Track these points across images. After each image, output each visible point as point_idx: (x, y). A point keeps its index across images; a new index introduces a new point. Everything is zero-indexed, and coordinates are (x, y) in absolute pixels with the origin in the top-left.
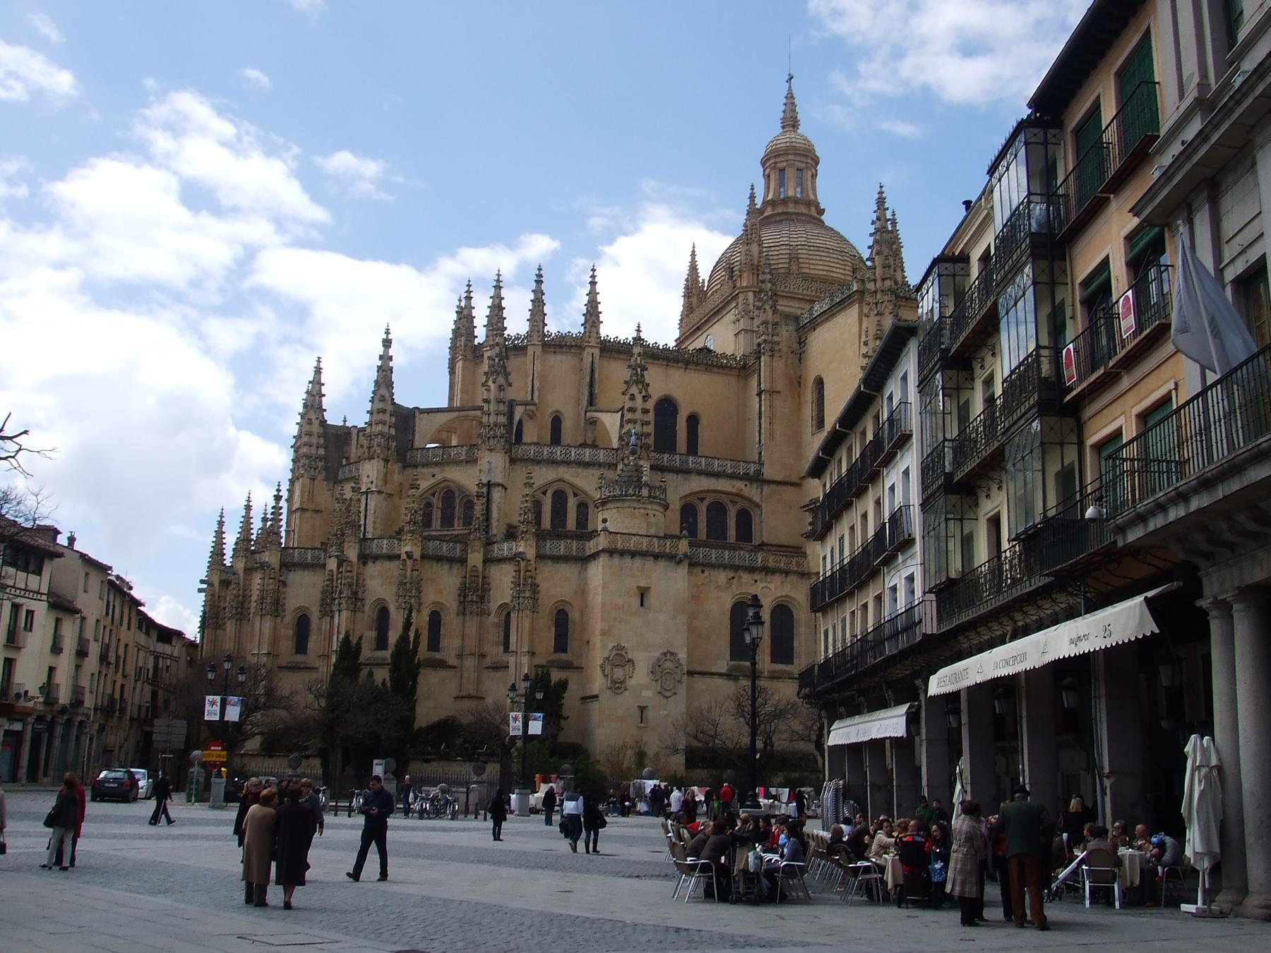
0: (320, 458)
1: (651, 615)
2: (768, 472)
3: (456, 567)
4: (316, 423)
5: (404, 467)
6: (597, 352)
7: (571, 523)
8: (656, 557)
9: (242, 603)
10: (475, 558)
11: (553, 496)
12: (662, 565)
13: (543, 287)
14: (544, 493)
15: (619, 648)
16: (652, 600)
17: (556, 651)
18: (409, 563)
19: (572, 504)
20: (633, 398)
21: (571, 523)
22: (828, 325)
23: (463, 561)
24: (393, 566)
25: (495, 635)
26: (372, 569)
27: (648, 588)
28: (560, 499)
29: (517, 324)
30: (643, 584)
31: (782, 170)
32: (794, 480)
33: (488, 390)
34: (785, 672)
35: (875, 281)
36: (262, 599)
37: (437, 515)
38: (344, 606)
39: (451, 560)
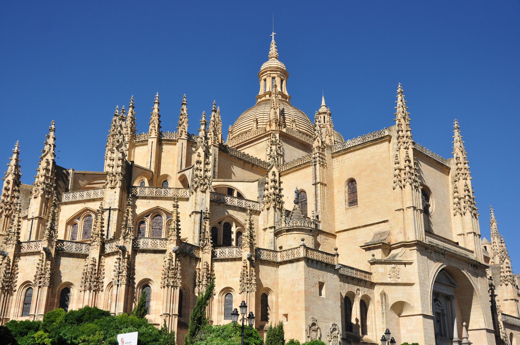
0: (52, 186)
4: (51, 162)
9: (12, 278)
10: (205, 256)
11: (224, 226)
14: (220, 223)
17: (262, 320)
18: (174, 255)
20: (274, 174)
22: (357, 152)
26: (139, 257)
30: (321, 280)
31: (274, 78)
32: (333, 233)
35: (402, 131)
36: (40, 276)
38: (124, 280)
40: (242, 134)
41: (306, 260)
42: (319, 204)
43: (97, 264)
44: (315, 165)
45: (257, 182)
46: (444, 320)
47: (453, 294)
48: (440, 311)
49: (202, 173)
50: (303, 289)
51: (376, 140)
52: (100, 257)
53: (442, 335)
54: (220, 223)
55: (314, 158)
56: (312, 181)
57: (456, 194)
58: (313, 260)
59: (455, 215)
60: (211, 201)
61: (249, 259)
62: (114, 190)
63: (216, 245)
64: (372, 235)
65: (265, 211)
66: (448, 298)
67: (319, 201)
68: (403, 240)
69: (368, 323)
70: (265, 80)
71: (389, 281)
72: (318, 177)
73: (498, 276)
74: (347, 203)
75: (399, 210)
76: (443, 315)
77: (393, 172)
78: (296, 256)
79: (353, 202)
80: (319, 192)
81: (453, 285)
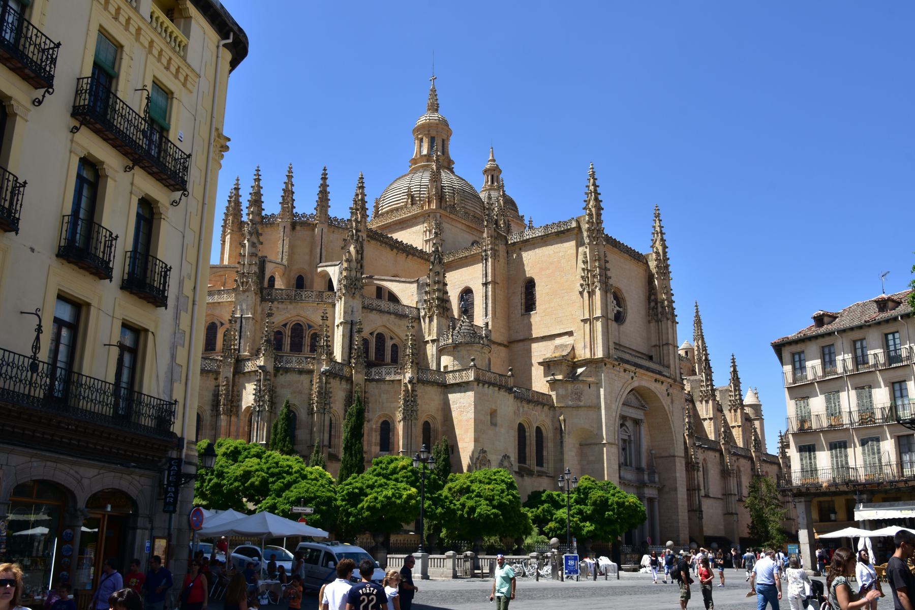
1: (497, 429)
2: (494, 337)
3: (344, 383)
5: (262, 301)
6: (365, 236)
7: (388, 357)
8: (500, 387)
12: (502, 392)
13: (328, 182)
15: (483, 451)
16: (499, 420)
19: (389, 344)
21: (388, 357)
23: (349, 380)
24: (304, 378)
25: (376, 438)
26: (282, 379)
27: (495, 411)
28: (380, 338)
29: (306, 205)
30: (494, 407)
32: (506, 343)
33: (349, 252)
34: (542, 472)
37: (287, 341)
39: (342, 378)
40: (392, 211)
41: (476, 384)
42: (490, 308)
43: (231, 383)
44: (486, 260)
45: (415, 285)
46: (630, 447)
47: (643, 417)
48: (626, 438)
49: (353, 273)
50: (472, 416)
51: (562, 232)
52: (234, 376)
53: (626, 465)
54: (371, 334)
55: (485, 251)
56: (481, 280)
57: (653, 297)
58: (484, 383)
59: (649, 322)
60: (363, 307)
61: (410, 382)
62: (247, 294)
63: (370, 365)
64: (552, 347)
65: (427, 320)
66: (637, 422)
67: (490, 305)
68: (588, 356)
69: (545, 453)
70: (421, 140)
71: (570, 403)
72: (490, 274)
73: (697, 390)
74: (523, 307)
75: (585, 321)
76: (630, 441)
77: (580, 273)
78: (465, 379)
79: (530, 304)
80: (490, 293)
81: (642, 407)
